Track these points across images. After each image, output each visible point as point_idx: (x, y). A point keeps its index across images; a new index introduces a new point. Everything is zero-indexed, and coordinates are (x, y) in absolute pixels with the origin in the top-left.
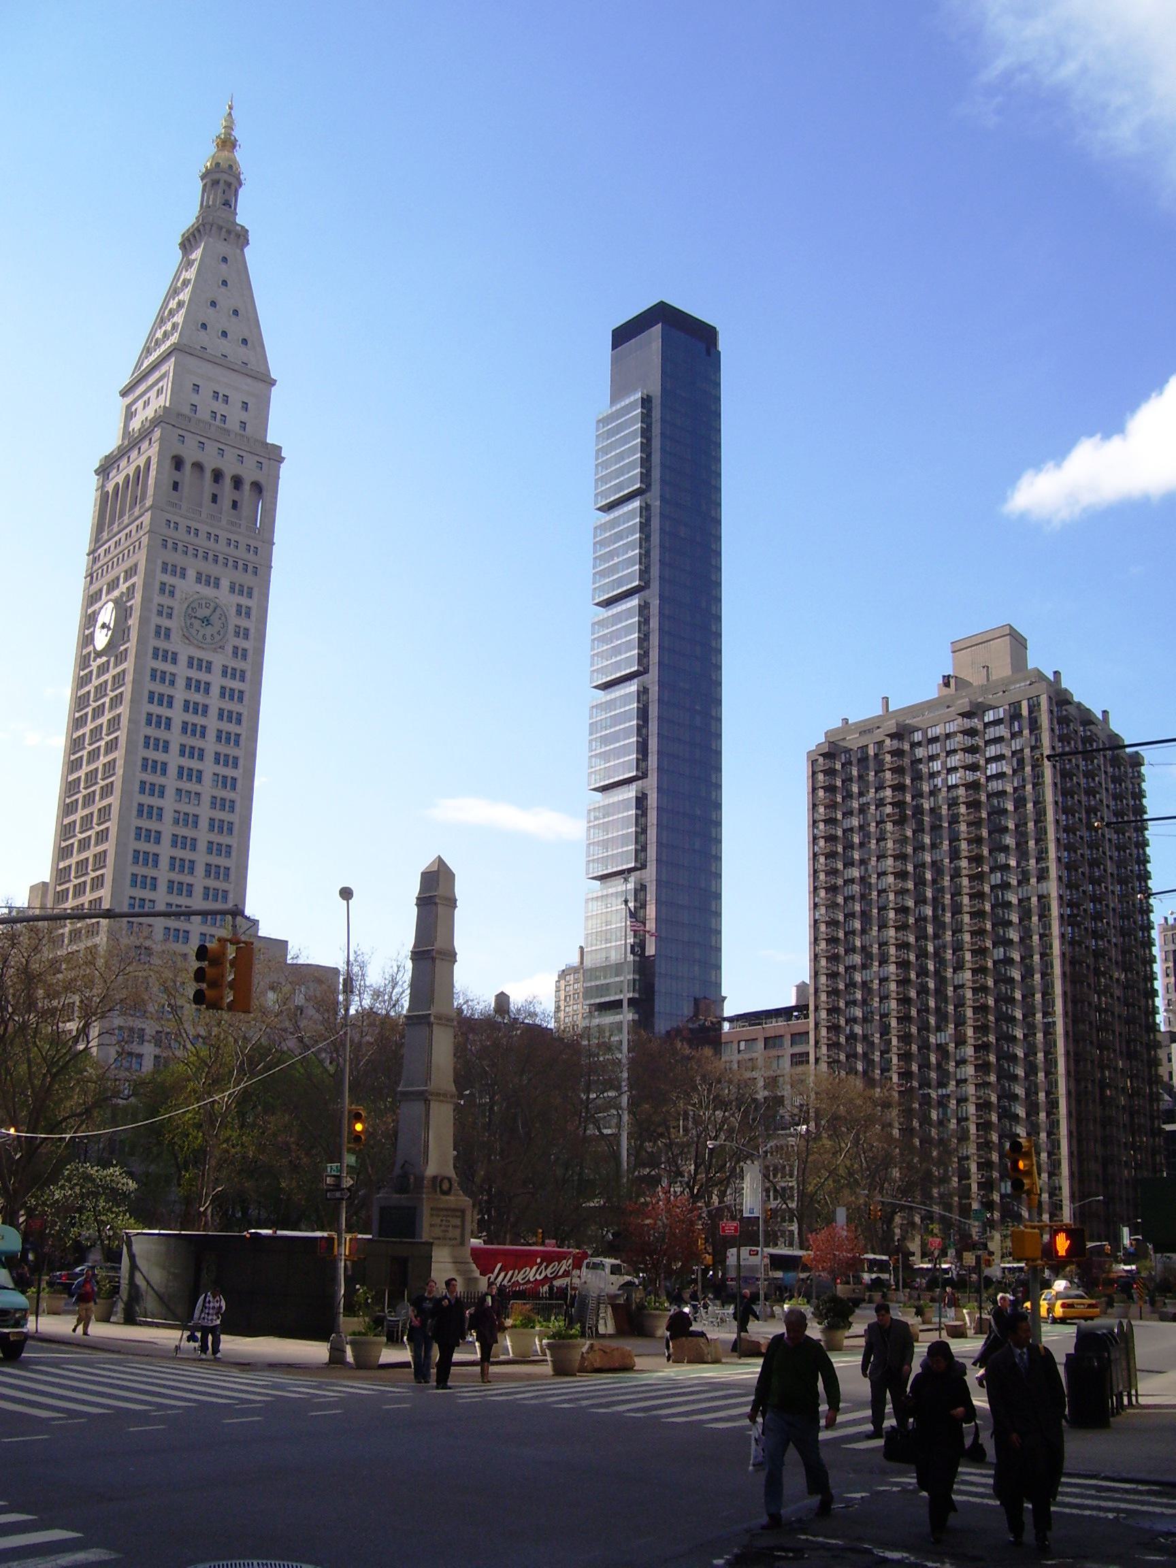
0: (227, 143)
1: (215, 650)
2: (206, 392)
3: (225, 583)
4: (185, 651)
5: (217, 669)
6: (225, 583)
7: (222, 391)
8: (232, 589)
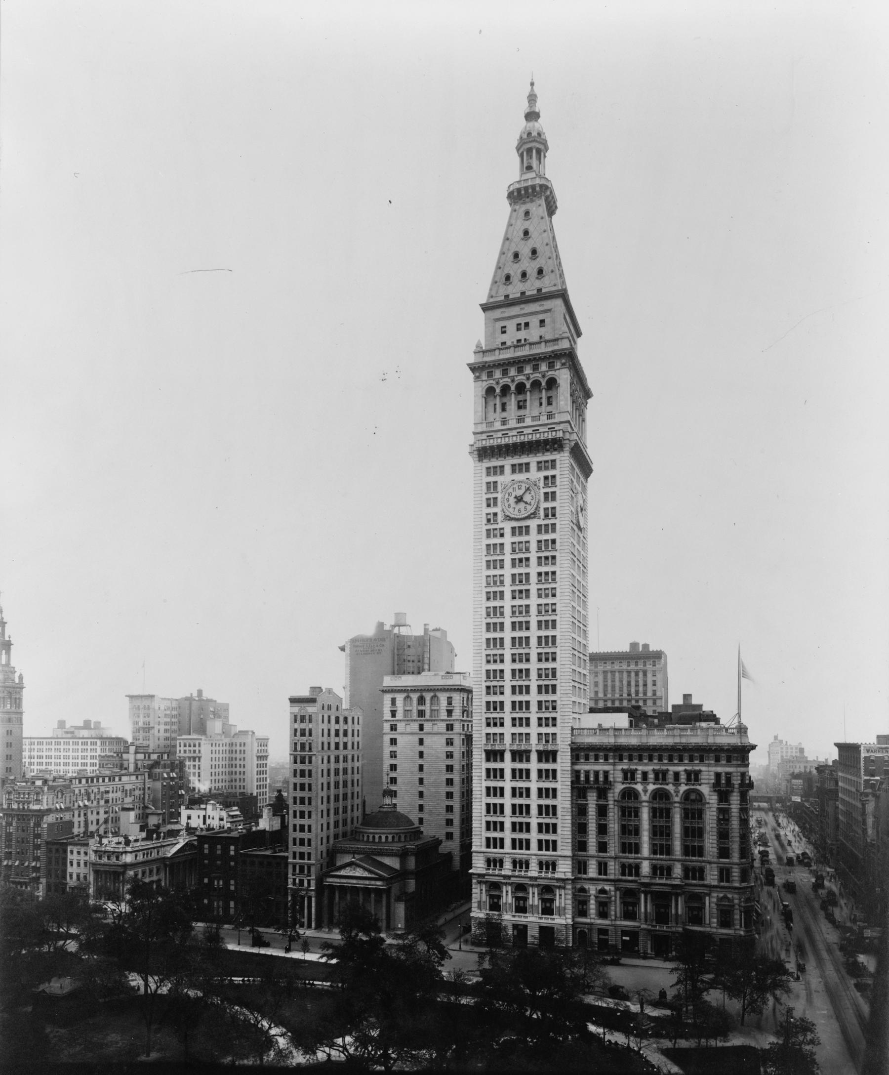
0: (532, 116)
1: (528, 517)
3: (533, 467)
4: (507, 526)
6: (533, 467)
7: (522, 321)
8: (539, 469)
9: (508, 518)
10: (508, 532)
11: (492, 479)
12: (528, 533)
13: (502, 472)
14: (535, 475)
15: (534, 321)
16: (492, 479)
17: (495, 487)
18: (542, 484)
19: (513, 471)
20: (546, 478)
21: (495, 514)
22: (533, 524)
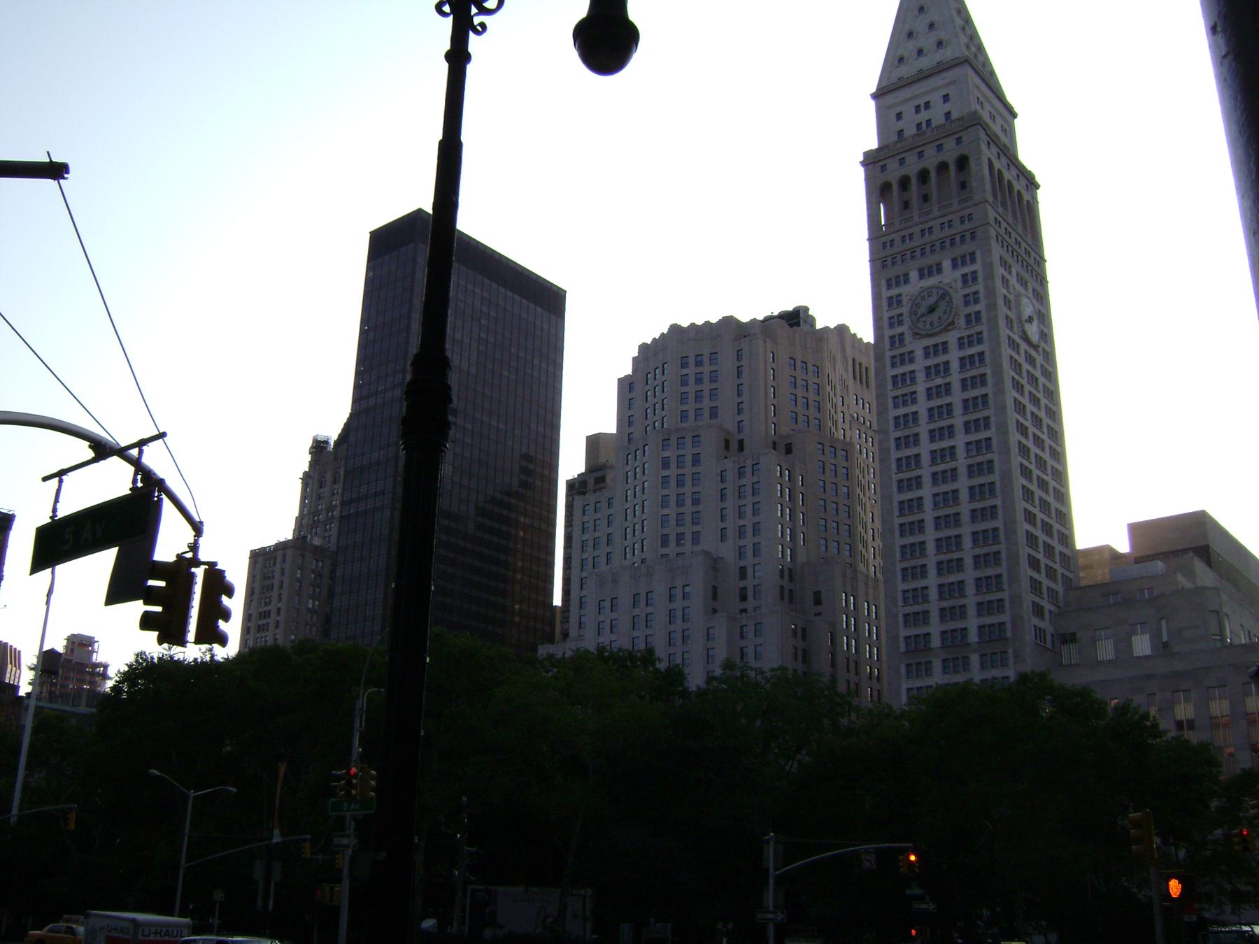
1: (946, 330)
2: (908, 110)
3: (947, 264)
4: (918, 347)
5: (953, 345)
6: (947, 264)
7: (921, 102)
8: (955, 266)
9: (917, 335)
10: (919, 353)
11: (894, 292)
12: (945, 350)
13: (907, 281)
14: (949, 276)
15: (936, 98)
16: (894, 292)
17: (899, 303)
18: (960, 284)
19: (921, 276)
20: (965, 276)
21: (902, 335)
22: (952, 337)
